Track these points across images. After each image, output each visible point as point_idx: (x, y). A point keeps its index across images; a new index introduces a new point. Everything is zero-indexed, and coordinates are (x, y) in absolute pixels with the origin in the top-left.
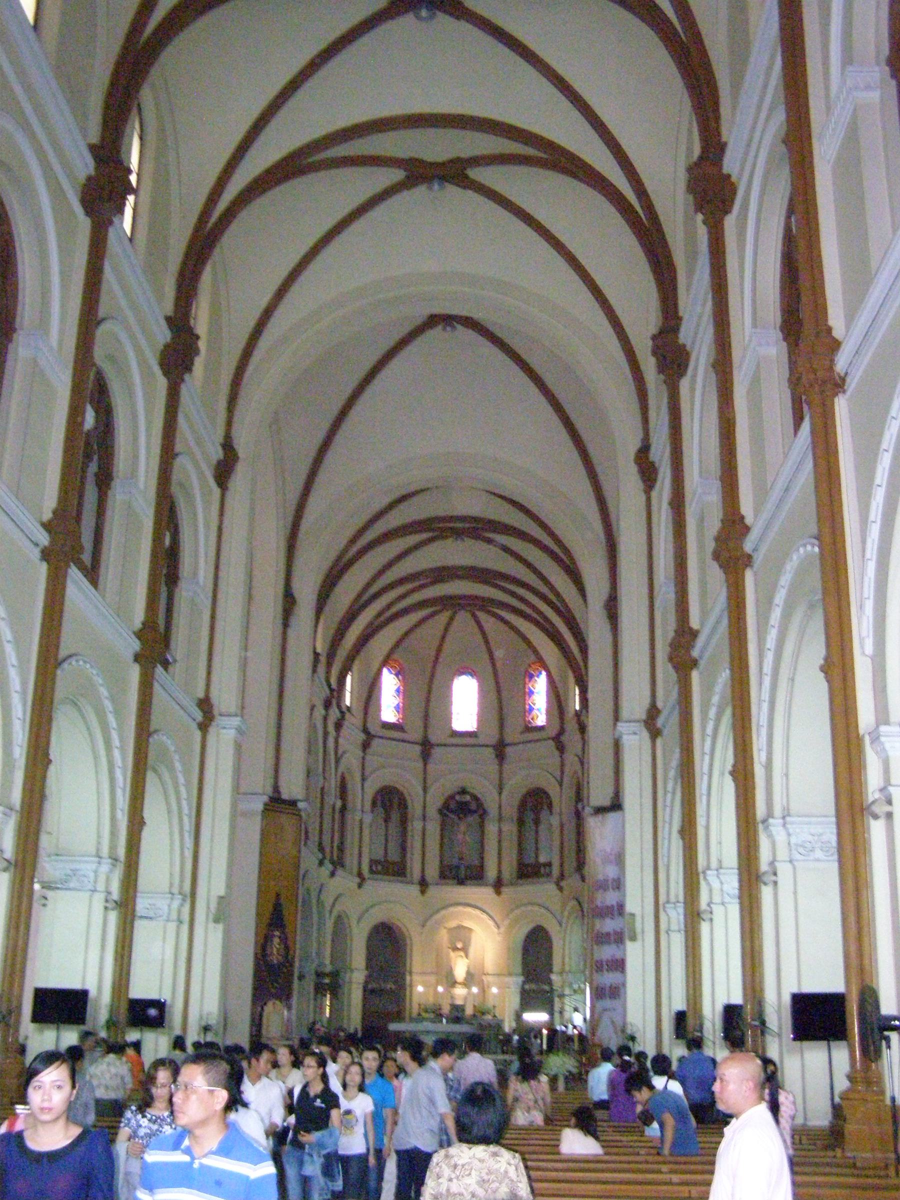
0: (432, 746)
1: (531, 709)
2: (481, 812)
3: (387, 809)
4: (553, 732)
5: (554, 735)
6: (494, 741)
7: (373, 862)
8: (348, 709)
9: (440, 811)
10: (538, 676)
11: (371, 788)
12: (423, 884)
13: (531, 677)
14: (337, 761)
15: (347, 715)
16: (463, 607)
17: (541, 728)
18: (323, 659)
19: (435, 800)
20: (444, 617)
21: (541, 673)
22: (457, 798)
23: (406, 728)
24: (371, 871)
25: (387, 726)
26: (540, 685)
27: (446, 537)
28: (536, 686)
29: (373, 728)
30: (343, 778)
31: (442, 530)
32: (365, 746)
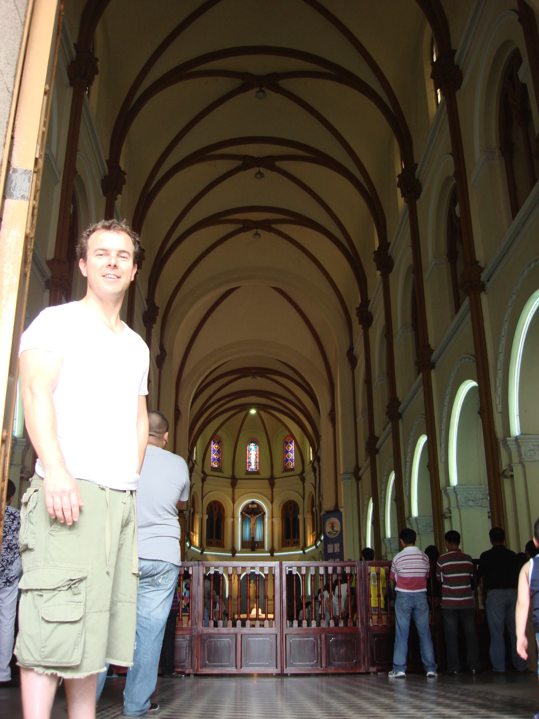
0: (237, 479)
2: (262, 513)
4: (298, 471)
5: (299, 473)
6: (268, 475)
9: (241, 513)
10: (291, 443)
11: (207, 500)
17: (293, 470)
21: (292, 442)
25: (213, 469)
29: (208, 471)
32: (203, 480)
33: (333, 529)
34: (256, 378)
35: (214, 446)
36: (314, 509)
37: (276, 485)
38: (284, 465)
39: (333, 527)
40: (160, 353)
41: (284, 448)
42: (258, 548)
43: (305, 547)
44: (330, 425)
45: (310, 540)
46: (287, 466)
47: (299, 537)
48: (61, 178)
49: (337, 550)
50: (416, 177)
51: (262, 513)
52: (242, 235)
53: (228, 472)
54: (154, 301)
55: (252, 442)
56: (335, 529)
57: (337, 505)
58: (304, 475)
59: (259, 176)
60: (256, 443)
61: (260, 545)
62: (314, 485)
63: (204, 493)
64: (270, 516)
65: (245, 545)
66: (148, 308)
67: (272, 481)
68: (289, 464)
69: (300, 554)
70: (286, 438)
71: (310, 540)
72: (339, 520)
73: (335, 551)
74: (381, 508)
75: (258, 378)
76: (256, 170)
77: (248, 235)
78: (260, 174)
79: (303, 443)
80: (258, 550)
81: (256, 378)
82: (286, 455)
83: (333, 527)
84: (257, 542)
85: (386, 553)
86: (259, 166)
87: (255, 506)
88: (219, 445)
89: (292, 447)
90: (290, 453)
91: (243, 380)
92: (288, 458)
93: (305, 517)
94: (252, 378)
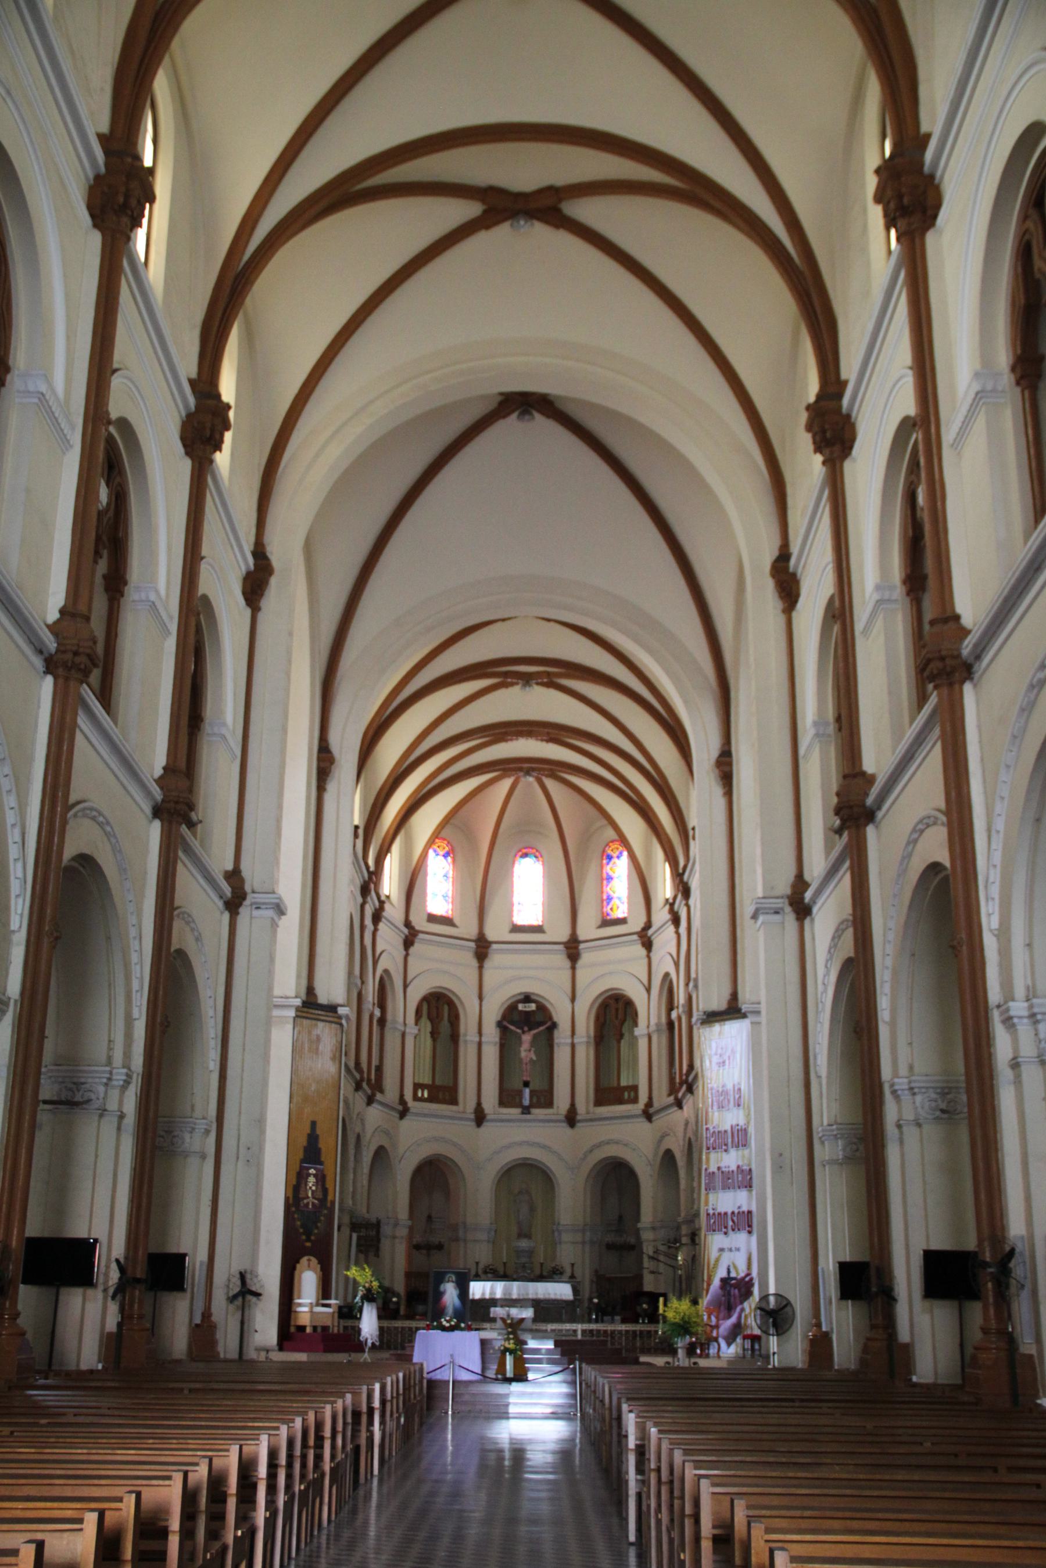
1: (610, 899)
2: (549, 1024)
3: (435, 1020)
4: (637, 924)
5: (638, 929)
6: (564, 935)
7: (417, 1086)
8: (388, 897)
9: (499, 1024)
10: (618, 857)
11: (417, 992)
12: (480, 1117)
13: (610, 858)
14: (375, 962)
15: (387, 906)
16: (528, 772)
17: (622, 921)
18: (361, 832)
19: (493, 1012)
20: (506, 784)
21: (621, 853)
22: (521, 1007)
23: (456, 921)
24: (416, 1098)
25: (432, 918)
26: (620, 868)
27: (512, 684)
28: (616, 869)
29: (419, 922)
30: (382, 979)
31: (506, 674)
44: (718, 791)
55: (525, 855)
57: (734, 996)
58: (650, 932)
60: (536, 857)
62: (675, 956)
63: (410, 975)
67: (573, 949)
68: (615, 908)
79: (649, 855)
82: (607, 886)
87: (533, 1007)
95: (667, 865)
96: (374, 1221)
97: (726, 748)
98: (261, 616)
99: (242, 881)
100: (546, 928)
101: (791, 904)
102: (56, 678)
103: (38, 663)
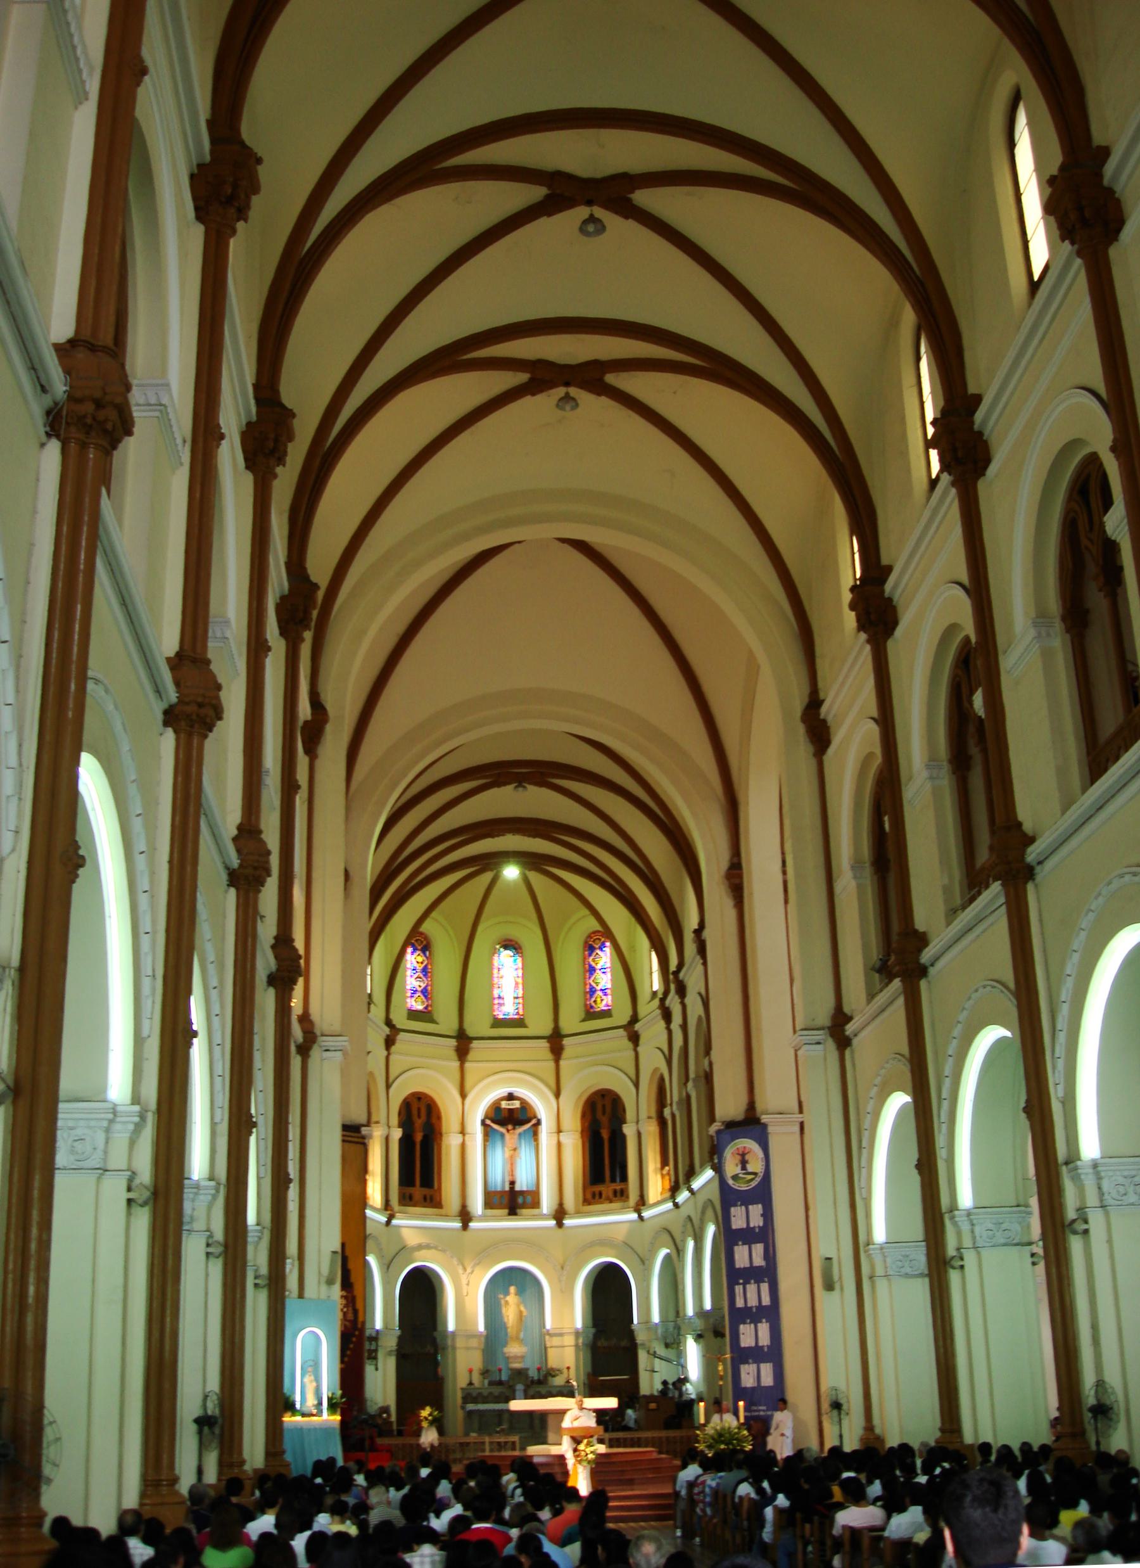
0: (471, 1039)
2: (534, 1121)
4: (622, 1016)
6: (546, 1029)
9: (483, 1123)
11: (399, 1093)
17: (606, 1014)
25: (413, 1015)
29: (400, 1020)
32: (389, 1042)
33: (744, 1168)
34: (525, 787)
35: (412, 959)
36: (667, 1112)
37: (566, 1053)
38: (586, 1005)
39: (744, 1163)
40: (313, 714)
41: (584, 962)
42: (524, 1206)
43: (642, 1203)
44: (729, 903)
45: (656, 1186)
46: (593, 1004)
47: (624, 1178)
48: (93, 86)
49: (757, 1221)
50: (1106, 182)
51: (534, 1121)
52: (527, 403)
53: (447, 1021)
54: (304, 569)
56: (750, 1168)
57: (751, 1106)
58: (637, 1026)
59: (591, 228)
60: (515, 949)
61: (529, 1199)
62: (666, 1049)
63: (393, 1073)
64: (554, 1129)
65: (492, 1200)
66: (290, 590)
67: (556, 1042)
68: (599, 1000)
69: (631, 1222)
70: (589, 937)
71: (656, 1186)
72: (760, 1145)
73: (752, 1225)
74: (940, 1127)
75: (532, 789)
76: (581, 212)
77: (542, 404)
78: (590, 227)
79: (633, 948)
80: (524, 1211)
81: (525, 787)
82: (590, 978)
83: (744, 1163)
84: (522, 1193)
85: (958, 1249)
86: (589, 203)
87: (516, 1104)
88: (425, 956)
89: (605, 958)
90: (598, 975)
91: (494, 791)
92: (594, 985)
93: (642, 1131)
94: (516, 787)
95: (654, 955)
96: (374, 1334)
97: (735, 860)
98: (318, 763)
99: (311, 1023)
100: (527, 1022)
101: (832, 1035)
102: (238, 890)
103: (224, 877)
